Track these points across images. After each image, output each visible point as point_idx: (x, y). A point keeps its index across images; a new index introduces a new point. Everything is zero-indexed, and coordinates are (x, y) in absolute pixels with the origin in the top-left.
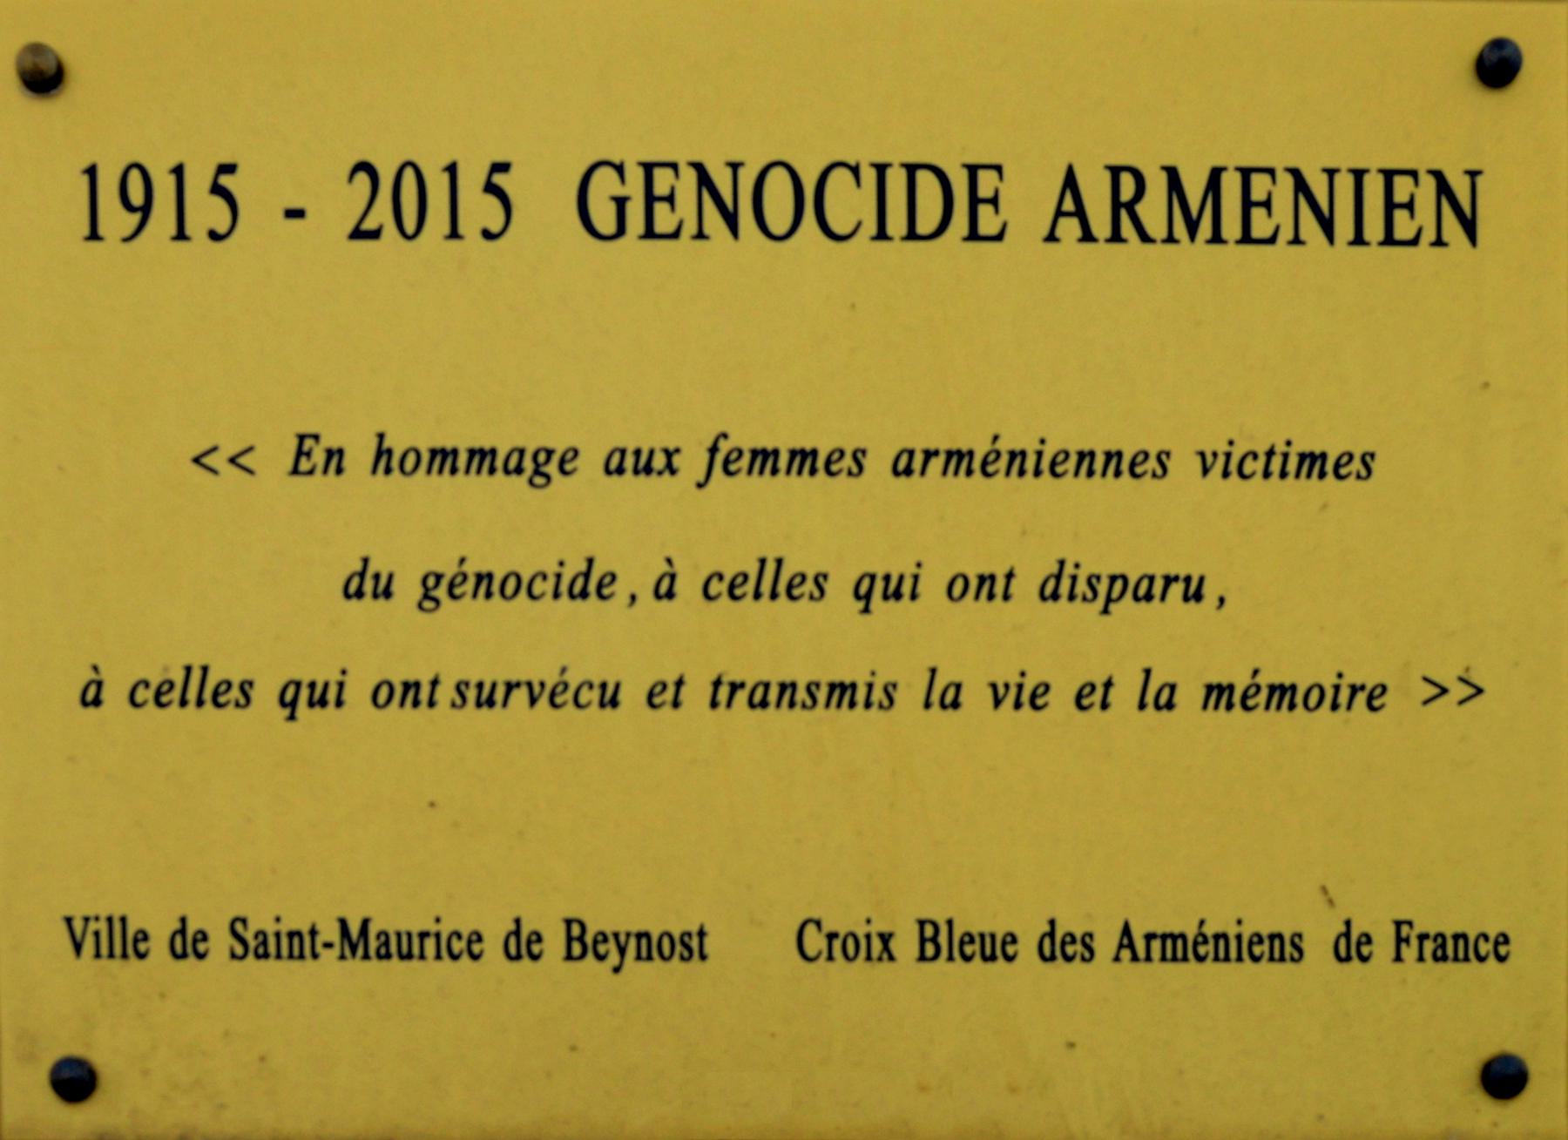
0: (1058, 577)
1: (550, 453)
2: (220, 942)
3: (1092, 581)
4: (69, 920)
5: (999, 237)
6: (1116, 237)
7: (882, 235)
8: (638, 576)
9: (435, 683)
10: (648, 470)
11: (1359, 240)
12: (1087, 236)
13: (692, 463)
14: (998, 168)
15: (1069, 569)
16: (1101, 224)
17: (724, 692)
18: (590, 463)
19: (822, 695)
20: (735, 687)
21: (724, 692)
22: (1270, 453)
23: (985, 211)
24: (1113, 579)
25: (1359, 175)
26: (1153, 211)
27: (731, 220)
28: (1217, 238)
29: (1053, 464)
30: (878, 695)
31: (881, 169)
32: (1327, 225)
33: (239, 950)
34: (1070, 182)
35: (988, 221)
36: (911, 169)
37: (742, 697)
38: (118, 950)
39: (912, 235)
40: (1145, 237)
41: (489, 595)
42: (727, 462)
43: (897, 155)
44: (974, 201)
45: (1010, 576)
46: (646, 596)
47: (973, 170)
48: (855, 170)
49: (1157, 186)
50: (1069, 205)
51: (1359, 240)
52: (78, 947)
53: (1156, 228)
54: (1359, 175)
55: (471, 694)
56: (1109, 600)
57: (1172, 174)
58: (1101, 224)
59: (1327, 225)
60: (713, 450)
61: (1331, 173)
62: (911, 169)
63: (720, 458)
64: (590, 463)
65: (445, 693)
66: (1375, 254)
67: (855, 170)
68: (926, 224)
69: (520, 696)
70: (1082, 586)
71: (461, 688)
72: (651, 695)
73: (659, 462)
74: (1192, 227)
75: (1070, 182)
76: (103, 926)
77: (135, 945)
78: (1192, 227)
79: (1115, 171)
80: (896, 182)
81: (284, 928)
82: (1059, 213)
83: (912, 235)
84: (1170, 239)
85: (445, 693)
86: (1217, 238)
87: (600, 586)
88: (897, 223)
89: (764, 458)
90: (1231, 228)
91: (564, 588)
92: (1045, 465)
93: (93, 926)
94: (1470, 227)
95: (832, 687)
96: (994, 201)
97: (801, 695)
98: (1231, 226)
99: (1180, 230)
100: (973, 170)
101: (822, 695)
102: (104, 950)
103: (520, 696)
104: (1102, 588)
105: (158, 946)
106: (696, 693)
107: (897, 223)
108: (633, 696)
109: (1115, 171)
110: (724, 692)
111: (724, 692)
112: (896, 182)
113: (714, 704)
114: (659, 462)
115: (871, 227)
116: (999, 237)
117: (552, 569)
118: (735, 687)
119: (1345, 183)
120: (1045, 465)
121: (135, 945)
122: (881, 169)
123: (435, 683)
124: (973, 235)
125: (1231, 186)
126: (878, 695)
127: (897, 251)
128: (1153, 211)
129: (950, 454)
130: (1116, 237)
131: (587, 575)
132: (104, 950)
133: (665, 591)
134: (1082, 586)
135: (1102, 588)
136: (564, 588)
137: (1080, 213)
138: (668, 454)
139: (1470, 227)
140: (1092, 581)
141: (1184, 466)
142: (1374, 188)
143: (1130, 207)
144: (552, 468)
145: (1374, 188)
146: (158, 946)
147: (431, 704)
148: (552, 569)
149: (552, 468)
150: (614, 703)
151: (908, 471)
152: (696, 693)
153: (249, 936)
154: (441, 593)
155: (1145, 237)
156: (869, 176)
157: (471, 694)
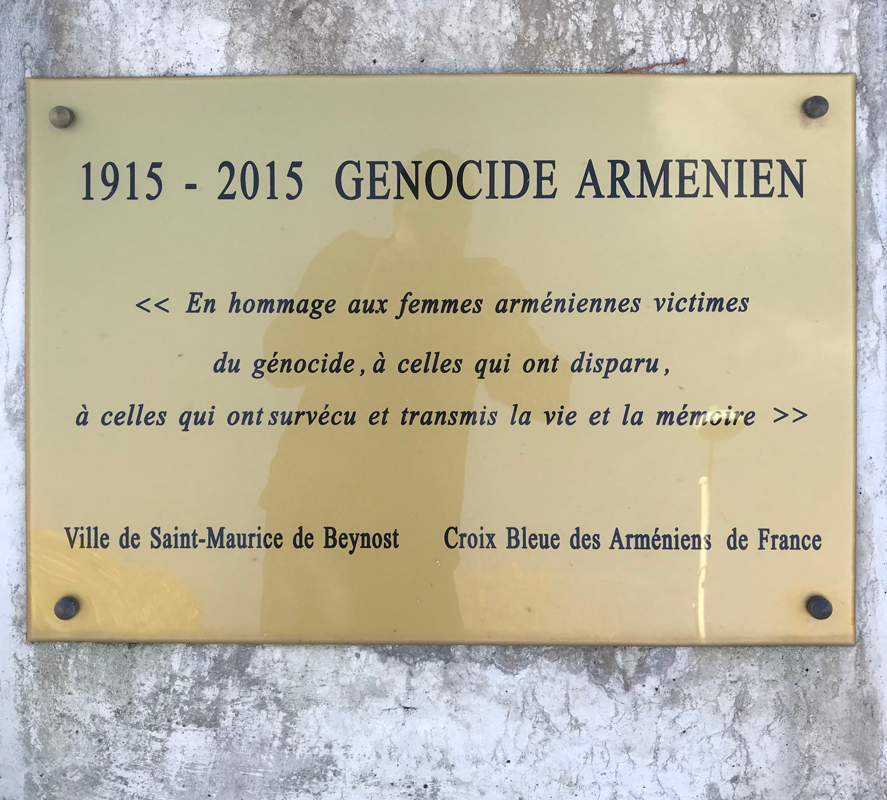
0: (581, 360)
1: (321, 302)
2: (146, 539)
3: (599, 362)
4: (67, 529)
5: (553, 196)
6: (614, 195)
7: (492, 195)
8: (364, 362)
9: (260, 412)
10: (371, 310)
11: (741, 194)
12: (599, 195)
13: (394, 307)
14: (553, 163)
15: (587, 357)
16: (606, 190)
17: (408, 416)
18: (341, 307)
19: (458, 418)
20: (414, 414)
21: (408, 417)
22: (693, 299)
23: (545, 184)
24: (610, 361)
25: (741, 163)
26: (633, 182)
27: (415, 190)
28: (666, 194)
29: (579, 306)
30: (487, 417)
31: (492, 164)
32: (724, 188)
33: (156, 543)
34: (590, 168)
35: (547, 189)
36: (508, 164)
37: (417, 419)
38: (93, 544)
39: (507, 195)
40: (629, 195)
41: (289, 370)
42: (411, 306)
43: (500, 156)
44: (540, 178)
45: (556, 360)
46: (369, 370)
47: (539, 164)
48: (479, 165)
49: (635, 170)
50: (589, 179)
51: (741, 194)
52: (72, 543)
53: (635, 190)
54: (741, 163)
55: (279, 418)
56: (607, 371)
57: (643, 164)
58: (606, 190)
59: (724, 188)
60: (404, 301)
61: (726, 162)
62: (508, 164)
63: (407, 304)
64: (341, 307)
65: (266, 418)
66: (749, 202)
67: (479, 165)
68: (515, 189)
69: (304, 419)
70: (593, 365)
71: (274, 415)
72: (371, 418)
73: (377, 306)
74: (653, 190)
75: (590, 168)
76: (85, 532)
77: (102, 541)
78: (653, 190)
79: (614, 163)
80: (500, 169)
81: (179, 532)
82: (584, 184)
83: (507, 195)
84: (642, 195)
85: (266, 418)
86: (666, 194)
87: (346, 366)
88: (500, 190)
89: (430, 305)
90: (674, 189)
91: (327, 367)
92: (575, 306)
93: (80, 532)
94: (799, 188)
95: (464, 414)
96: (550, 179)
97: (448, 418)
98: (674, 189)
99: (647, 191)
100: (539, 164)
101: (458, 418)
102: (86, 544)
103: (304, 419)
104: (604, 366)
105: (114, 541)
106: (394, 417)
107: (500, 190)
108: (362, 419)
109: (614, 163)
110: (408, 416)
111: (408, 417)
112: (500, 169)
113: (403, 423)
114: (377, 306)
115: (486, 192)
116: (553, 196)
117: (321, 358)
118: (414, 414)
119: (733, 167)
120: (575, 306)
121: (102, 541)
122: (492, 164)
123: (260, 412)
124: (539, 195)
125: (674, 169)
126: (487, 417)
127: (501, 203)
128: (633, 182)
129: (525, 301)
130: (614, 195)
131: (339, 361)
132: (86, 544)
133: (379, 367)
134: (593, 365)
135: (604, 366)
136: (327, 367)
137: (595, 183)
138: (382, 303)
139: (799, 188)
140: (599, 362)
141: (648, 305)
142: (749, 168)
143: (621, 180)
144: (322, 309)
145: (749, 168)
146: (114, 541)
147: (258, 423)
148: (321, 358)
149: (322, 309)
150: (352, 422)
151: (504, 310)
152: (394, 417)
153: (161, 537)
154: (264, 369)
155: (629, 195)
156: (486, 167)
157: (279, 418)
